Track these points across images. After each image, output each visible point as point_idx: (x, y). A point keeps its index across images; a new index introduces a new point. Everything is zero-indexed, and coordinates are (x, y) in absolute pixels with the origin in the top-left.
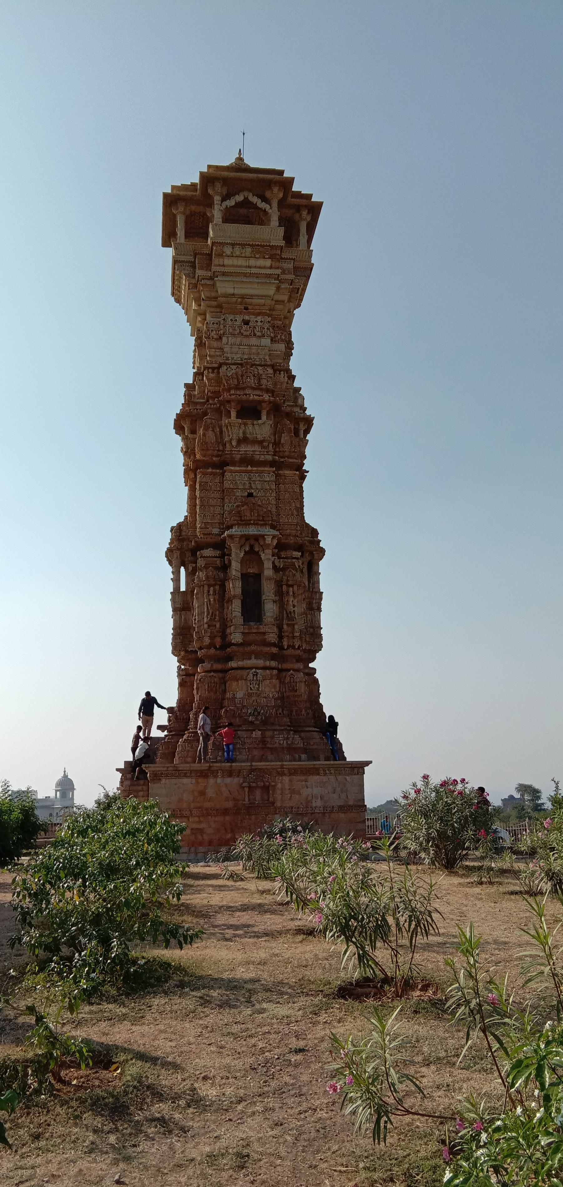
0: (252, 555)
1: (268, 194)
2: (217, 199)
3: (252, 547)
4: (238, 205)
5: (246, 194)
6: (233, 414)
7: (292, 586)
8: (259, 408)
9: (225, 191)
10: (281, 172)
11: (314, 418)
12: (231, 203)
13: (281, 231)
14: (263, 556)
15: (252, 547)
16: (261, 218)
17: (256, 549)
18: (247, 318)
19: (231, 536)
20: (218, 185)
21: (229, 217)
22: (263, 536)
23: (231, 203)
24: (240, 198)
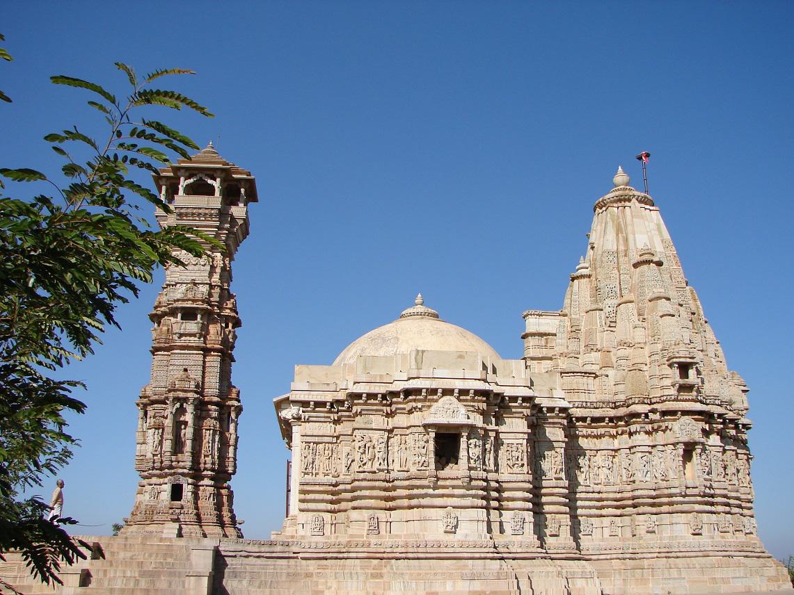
1: (215, 175)
3: (182, 405)
6: (179, 315)
9: (187, 174)
15: (182, 405)
16: (210, 191)
21: (190, 190)
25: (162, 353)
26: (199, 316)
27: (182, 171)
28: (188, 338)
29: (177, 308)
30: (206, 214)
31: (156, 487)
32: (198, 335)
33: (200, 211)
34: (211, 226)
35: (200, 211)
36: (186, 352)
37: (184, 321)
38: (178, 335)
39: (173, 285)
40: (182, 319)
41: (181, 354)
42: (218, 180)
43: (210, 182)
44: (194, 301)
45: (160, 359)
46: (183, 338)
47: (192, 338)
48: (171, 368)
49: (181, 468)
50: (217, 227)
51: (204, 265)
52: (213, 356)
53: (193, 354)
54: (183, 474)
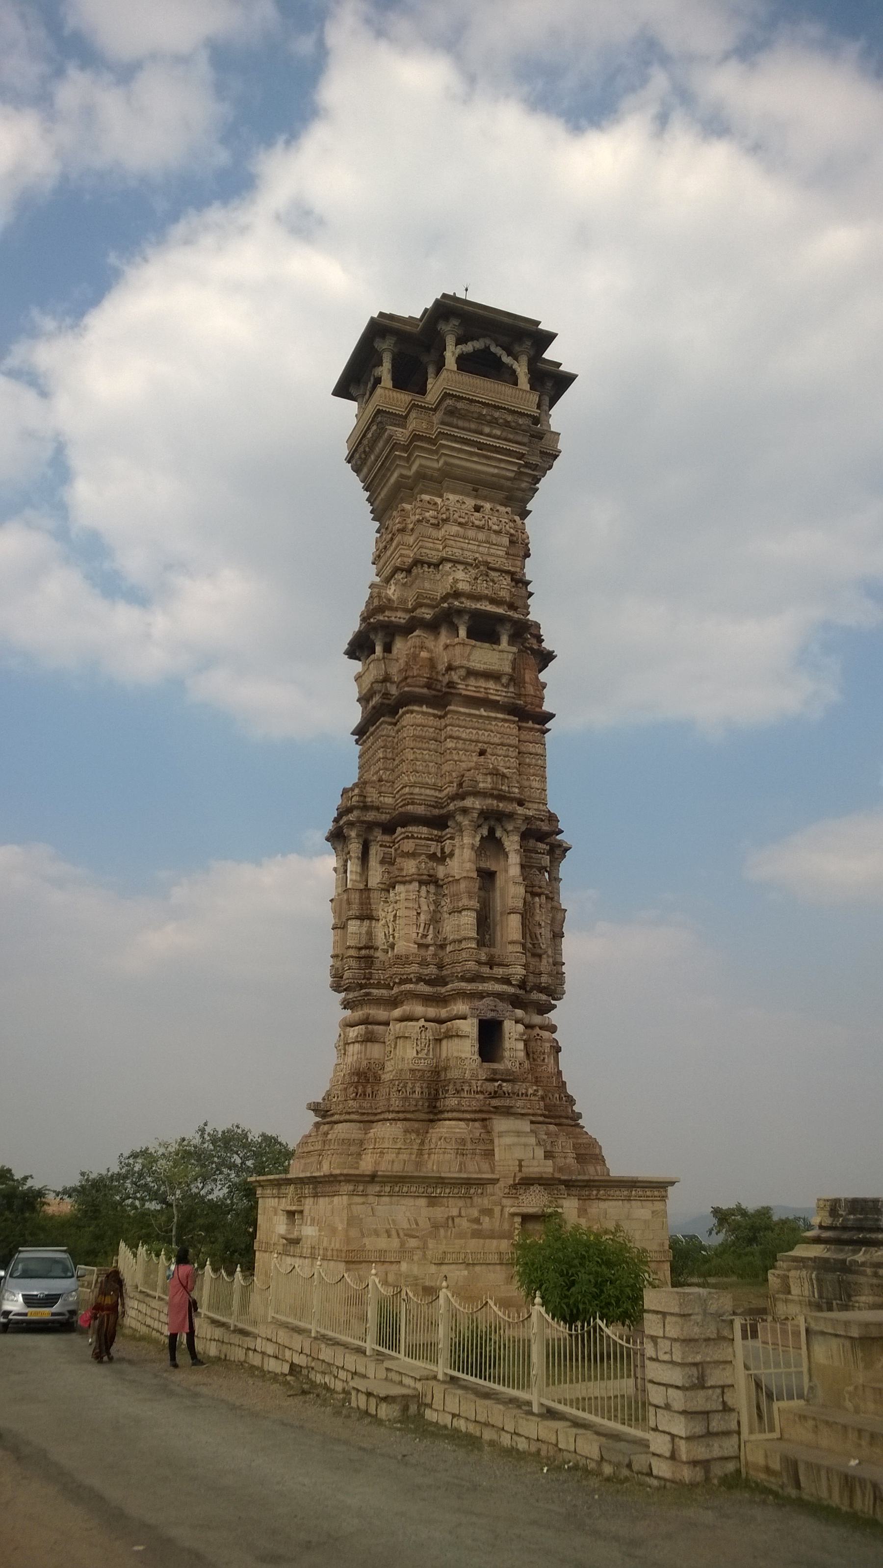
0: (491, 844)
1: (517, 348)
2: (450, 341)
3: (492, 831)
4: (476, 353)
5: (488, 341)
6: (463, 633)
7: (539, 895)
8: (499, 628)
10: (539, 323)
11: (556, 656)
12: (469, 347)
13: (535, 397)
14: (506, 844)
15: (492, 831)
17: (498, 834)
18: (480, 503)
19: (465, 811)
20: (455, 322)
22: (511, 816)
23: (469, 347)
24: (478, 345)
25: (424, 709)
26: (504, 639)
27: (455, 322)
28: (482, 683)
29: (460, 612)
30: (507, 424)
31: (427, 1024)
32: (504, 680)
33: (497, 414)
34: (509, 453)
35: (497, 414)
36: (482, 712)
37: (473, 642)
38: (463, 672)
39: (430, 565)
40: (469, 635)
41: (470, 715)
42: (524, 360)
43: (506, 359)
44: (493, 601)
45: (419, 721)
46: (472, 681)
47: (491, 685)
48: (450, 744)
49: (497, 980)
50: (521, 456)
51: (498, 532)
52: (531, 729)
53: (496, 718)
54: (499, 996)
